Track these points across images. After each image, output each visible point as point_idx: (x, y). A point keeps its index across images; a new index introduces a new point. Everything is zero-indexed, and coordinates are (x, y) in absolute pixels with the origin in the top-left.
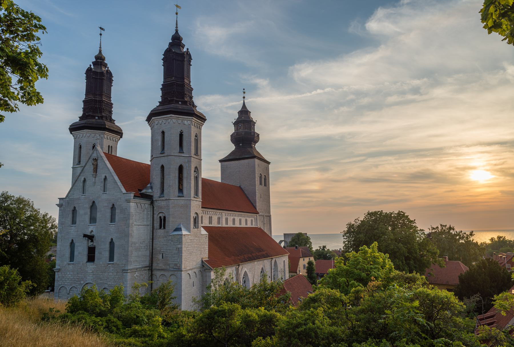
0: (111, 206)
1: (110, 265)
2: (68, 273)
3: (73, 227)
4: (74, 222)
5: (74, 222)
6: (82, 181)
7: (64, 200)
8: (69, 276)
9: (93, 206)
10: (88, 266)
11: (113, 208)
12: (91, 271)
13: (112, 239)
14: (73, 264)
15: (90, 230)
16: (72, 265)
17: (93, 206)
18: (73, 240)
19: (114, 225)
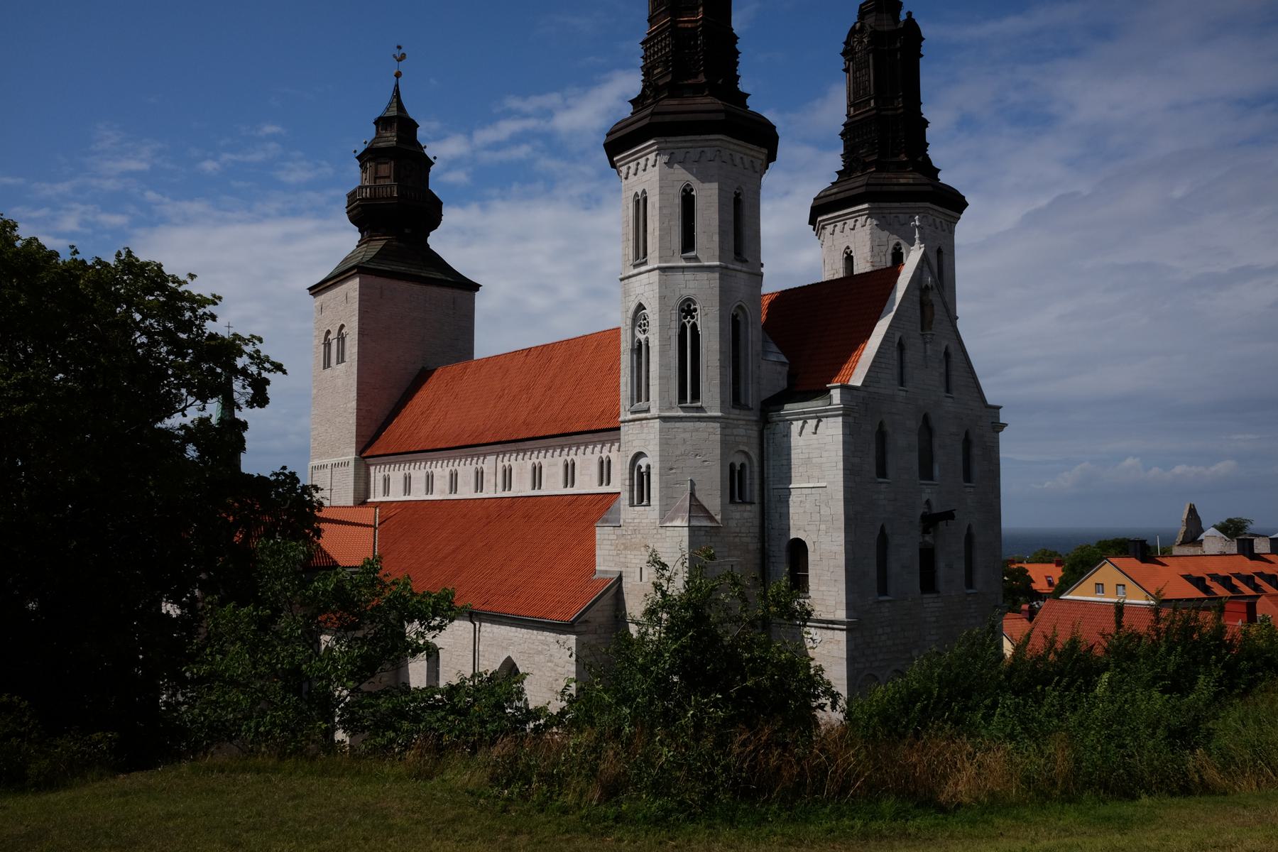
0: (963, 436)
1: (969, 599)
2: (880, 631)
3: (884, 486)
4: (882, 471)
5: (882, 471)
6: (896, 346)
7: (855, 392)
8: (884, 638)
9: (927, 428)
10: (925, 606)
11: (967, 443)
12: (934, 619)
13: (969, 528)
14: (889, 601)
15: (925, 497)
16: (887, 604)
17: (927, 428)
18: (883, 528)
19: (972, 490)
